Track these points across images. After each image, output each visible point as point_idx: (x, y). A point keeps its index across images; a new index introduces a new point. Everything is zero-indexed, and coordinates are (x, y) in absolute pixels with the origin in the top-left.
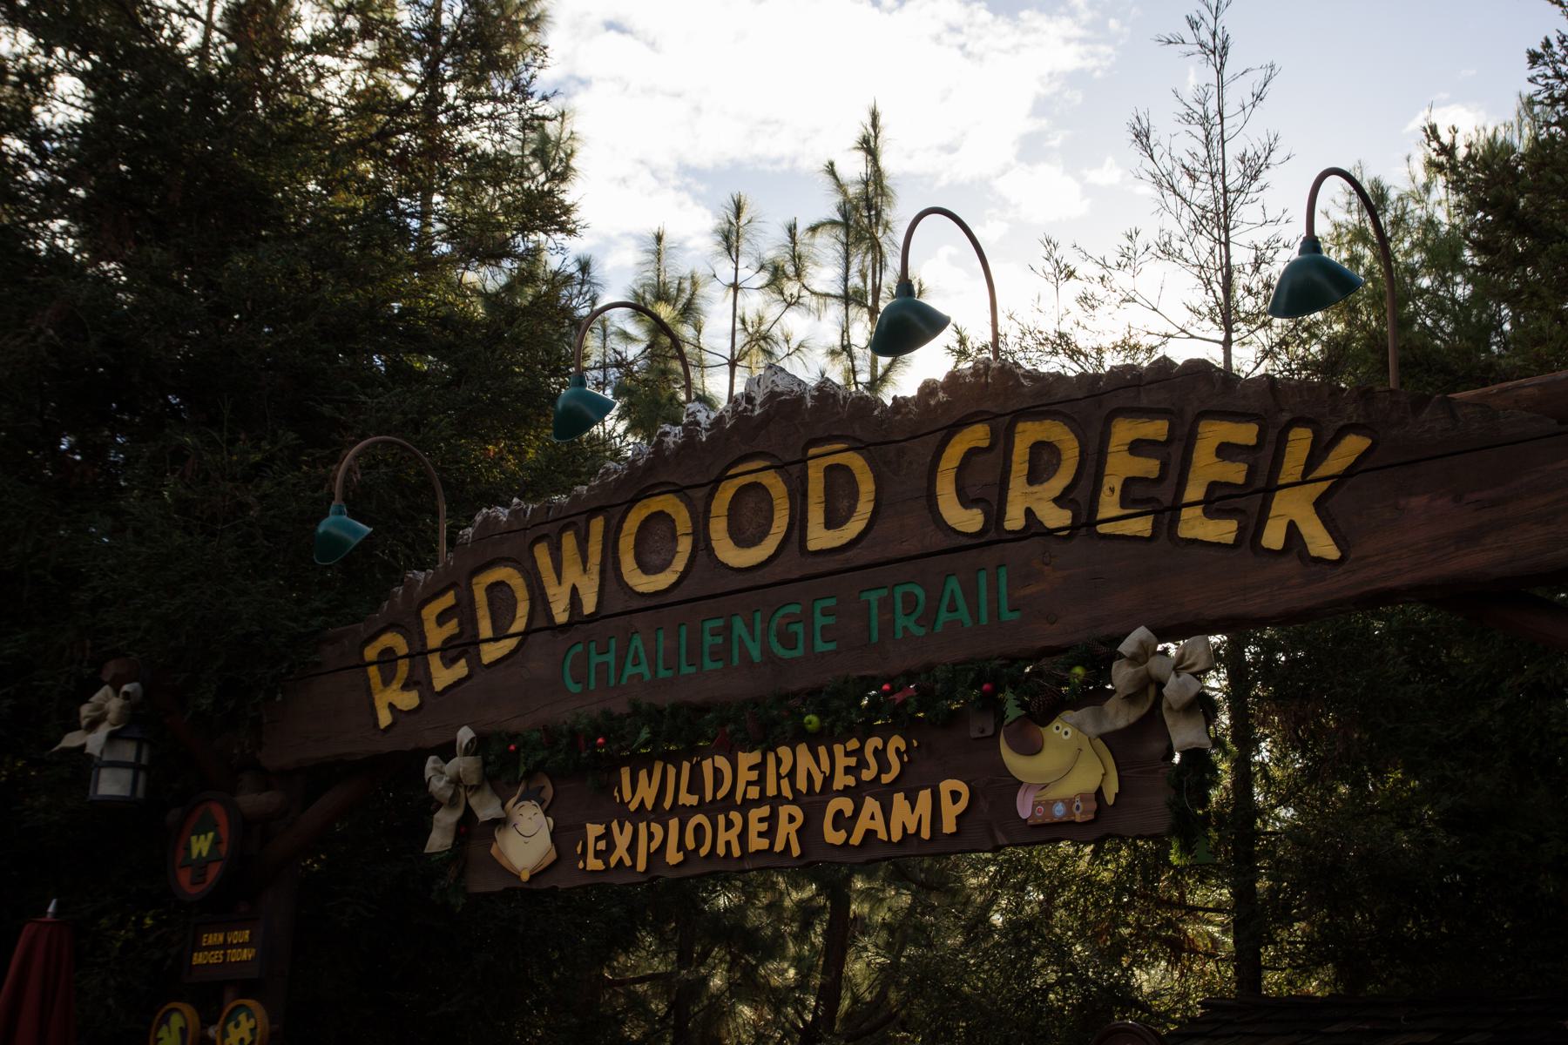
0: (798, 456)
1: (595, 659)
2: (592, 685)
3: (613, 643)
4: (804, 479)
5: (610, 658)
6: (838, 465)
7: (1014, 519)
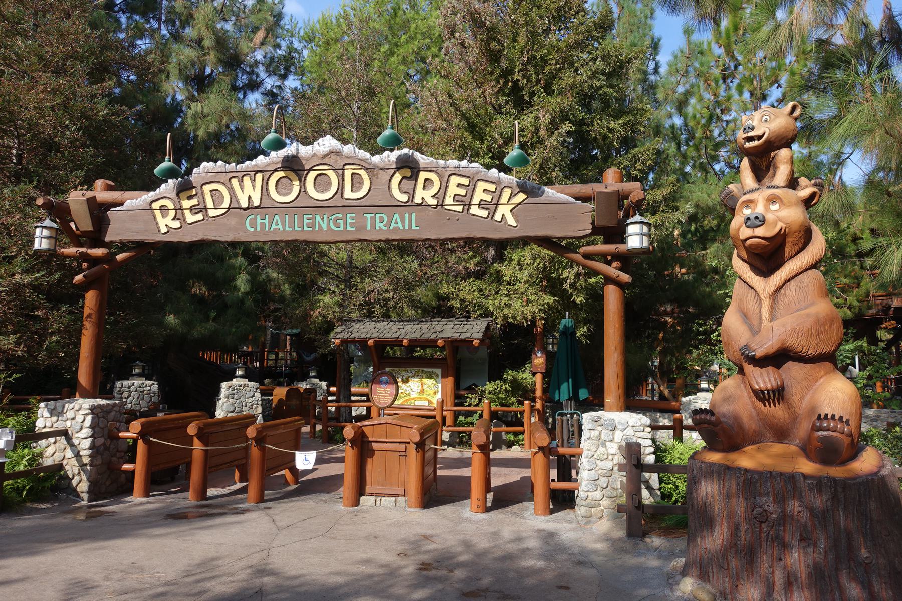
0: (341, 167)
1: (259, 221)
2: (258, 229)
3: (267, 217)
4: (343, 175)
5: (266, 222)
6: (358, 174)
7: (418, 200)
